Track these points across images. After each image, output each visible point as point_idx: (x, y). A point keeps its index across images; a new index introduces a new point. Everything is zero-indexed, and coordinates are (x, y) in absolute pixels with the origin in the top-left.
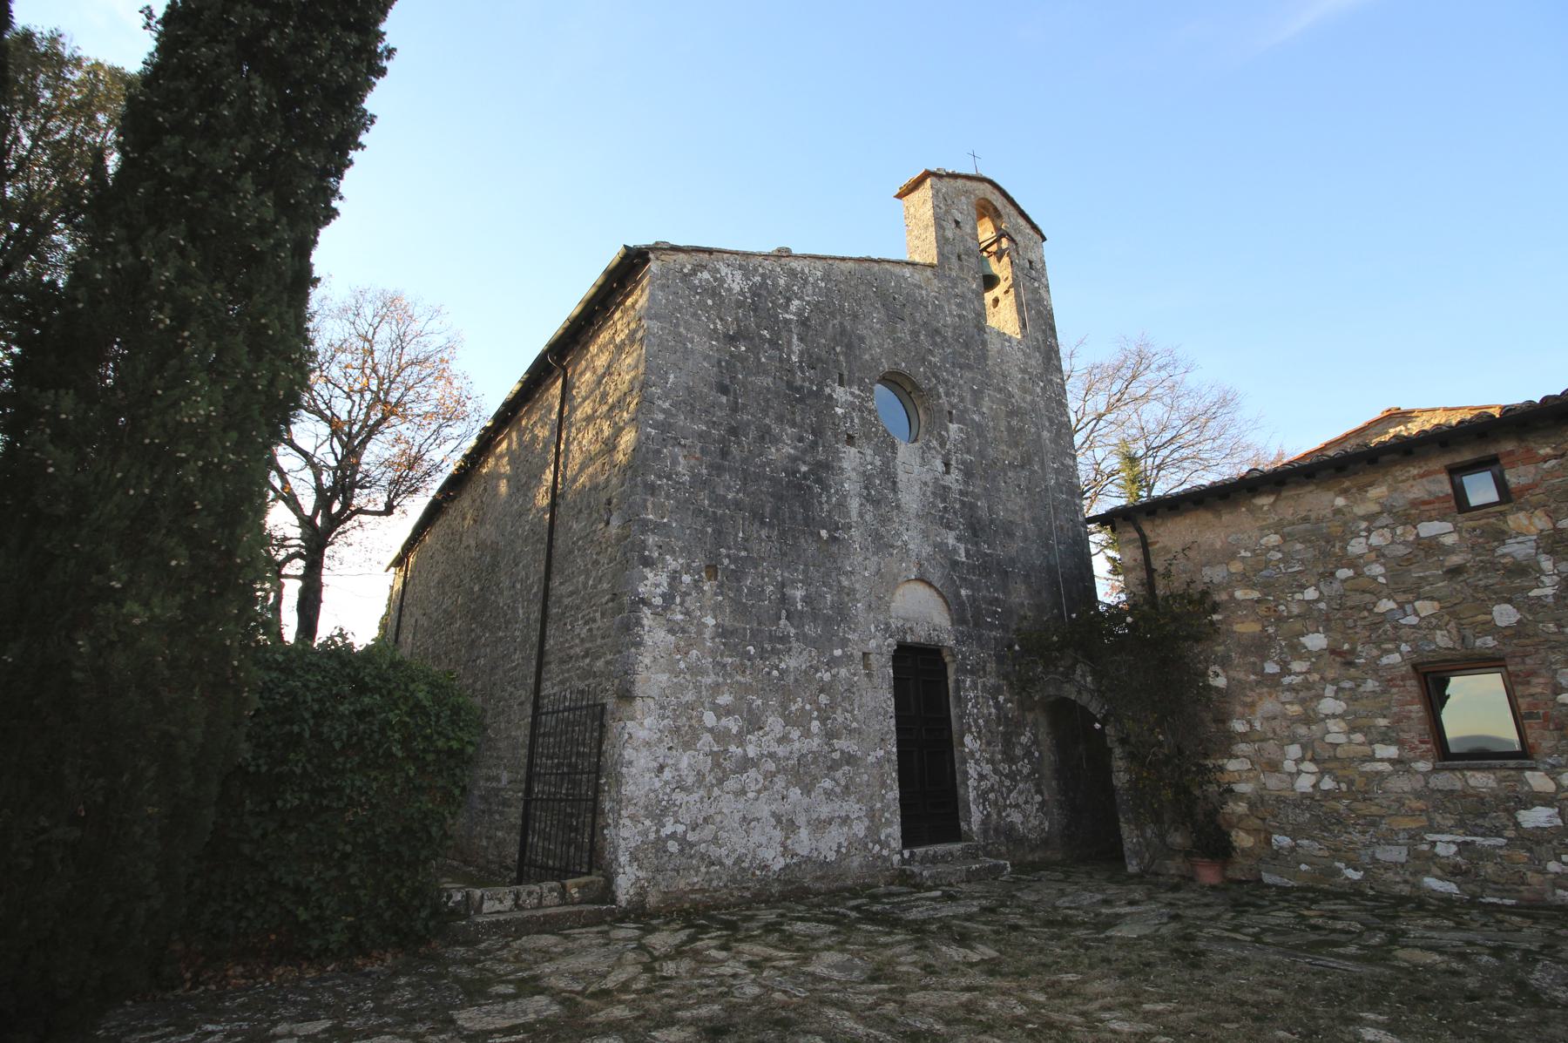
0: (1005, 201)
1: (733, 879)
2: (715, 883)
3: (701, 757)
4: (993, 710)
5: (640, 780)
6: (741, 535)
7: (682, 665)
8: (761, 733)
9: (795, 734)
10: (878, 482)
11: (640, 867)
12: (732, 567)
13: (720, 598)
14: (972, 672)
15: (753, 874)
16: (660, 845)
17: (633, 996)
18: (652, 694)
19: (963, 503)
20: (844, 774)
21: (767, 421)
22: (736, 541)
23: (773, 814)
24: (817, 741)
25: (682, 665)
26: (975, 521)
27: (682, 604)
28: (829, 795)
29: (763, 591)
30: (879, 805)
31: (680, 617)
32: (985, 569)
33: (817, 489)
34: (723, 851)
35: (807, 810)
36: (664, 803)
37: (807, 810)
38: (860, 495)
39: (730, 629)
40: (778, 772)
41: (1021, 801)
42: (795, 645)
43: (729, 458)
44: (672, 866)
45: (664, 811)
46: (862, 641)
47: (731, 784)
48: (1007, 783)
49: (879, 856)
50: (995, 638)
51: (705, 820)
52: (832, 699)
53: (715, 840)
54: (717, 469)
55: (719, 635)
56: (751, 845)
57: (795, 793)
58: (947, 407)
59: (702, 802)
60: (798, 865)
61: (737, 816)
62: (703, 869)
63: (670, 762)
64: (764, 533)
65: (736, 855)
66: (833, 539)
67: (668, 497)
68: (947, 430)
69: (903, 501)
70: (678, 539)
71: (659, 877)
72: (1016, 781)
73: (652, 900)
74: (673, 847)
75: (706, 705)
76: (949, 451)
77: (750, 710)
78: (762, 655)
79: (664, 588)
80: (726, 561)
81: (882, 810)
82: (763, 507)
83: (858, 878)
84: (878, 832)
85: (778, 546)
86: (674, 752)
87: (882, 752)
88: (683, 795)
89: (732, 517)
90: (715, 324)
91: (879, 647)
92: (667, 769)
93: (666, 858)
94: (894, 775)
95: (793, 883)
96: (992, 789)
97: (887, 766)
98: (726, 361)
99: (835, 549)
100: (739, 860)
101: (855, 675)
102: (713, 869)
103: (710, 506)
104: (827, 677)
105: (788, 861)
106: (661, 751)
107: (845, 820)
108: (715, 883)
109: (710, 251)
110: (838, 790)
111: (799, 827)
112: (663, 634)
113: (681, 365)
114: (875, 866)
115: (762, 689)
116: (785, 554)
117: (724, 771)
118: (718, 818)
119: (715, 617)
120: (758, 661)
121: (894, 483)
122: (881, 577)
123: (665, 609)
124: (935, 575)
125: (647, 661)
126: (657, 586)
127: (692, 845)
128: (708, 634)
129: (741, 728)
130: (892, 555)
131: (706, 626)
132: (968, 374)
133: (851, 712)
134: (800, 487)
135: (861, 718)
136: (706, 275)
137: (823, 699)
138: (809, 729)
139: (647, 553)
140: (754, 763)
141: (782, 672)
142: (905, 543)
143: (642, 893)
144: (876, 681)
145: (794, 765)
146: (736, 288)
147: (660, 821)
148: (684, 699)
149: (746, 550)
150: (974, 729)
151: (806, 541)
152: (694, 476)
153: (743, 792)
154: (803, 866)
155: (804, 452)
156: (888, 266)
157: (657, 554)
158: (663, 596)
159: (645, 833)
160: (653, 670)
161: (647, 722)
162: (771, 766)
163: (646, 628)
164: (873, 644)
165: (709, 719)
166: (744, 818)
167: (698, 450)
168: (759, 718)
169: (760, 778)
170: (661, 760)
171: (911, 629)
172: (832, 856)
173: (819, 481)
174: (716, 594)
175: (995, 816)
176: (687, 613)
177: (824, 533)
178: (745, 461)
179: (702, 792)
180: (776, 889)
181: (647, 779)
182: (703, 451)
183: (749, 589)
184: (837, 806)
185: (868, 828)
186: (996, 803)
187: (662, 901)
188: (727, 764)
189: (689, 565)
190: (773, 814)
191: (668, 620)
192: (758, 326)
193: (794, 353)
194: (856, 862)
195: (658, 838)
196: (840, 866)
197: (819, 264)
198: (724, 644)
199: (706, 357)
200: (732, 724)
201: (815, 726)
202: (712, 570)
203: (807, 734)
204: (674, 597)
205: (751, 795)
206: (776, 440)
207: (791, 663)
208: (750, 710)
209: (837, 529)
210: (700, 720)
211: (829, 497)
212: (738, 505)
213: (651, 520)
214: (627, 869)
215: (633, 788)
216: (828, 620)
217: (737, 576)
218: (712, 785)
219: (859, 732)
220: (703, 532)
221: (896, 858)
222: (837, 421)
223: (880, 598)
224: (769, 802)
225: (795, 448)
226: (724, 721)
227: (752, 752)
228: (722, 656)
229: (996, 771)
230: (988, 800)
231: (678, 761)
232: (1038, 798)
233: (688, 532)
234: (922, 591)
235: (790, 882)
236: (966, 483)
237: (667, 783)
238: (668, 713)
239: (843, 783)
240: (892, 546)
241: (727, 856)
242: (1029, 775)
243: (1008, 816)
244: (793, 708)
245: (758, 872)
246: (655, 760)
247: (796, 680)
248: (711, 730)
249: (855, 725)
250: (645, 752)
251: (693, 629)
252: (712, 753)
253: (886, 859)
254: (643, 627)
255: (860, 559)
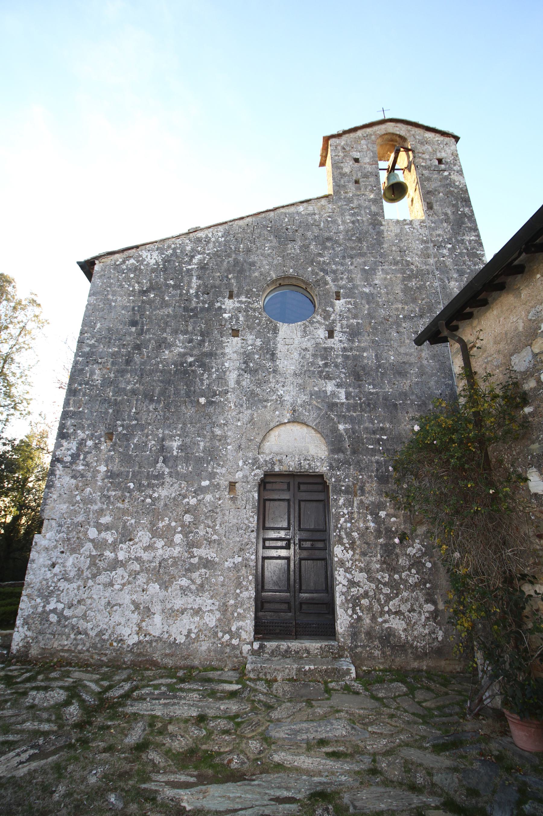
0: (409, 127)
1: (94, 646)
2: (80, 647)
3: (82, 558)
4: (372, 525)
5: (38, 572)
6: (134, 410)
7: (78, 498)
8: (131, 543)
9: (160, 543)
10: (257, 356)
11: (29, 629)
12: (125, 432)
13: (112, 453)
14: (347, 492)
15: (111, 645)
16: (44, 616)
17: (151, 683)
18: (54, 517)
19: (346, 357)
20: (200, 575)
21: (165, 335)
22: (129, 415)
23: (133, 602)
24: (178, 549)
25: (78, 498)
26: (358, 369)
27: (84, 460)
28: (185, 591)
29: (146, 445)
30: (232, 602)
31: (81, 467)
32: (369, 405)
33: (200, 371)
34: (90, 625)
35: (163, 601)
36: (51, 588)
37: (163, 601)
38: (239, 369)
39: (117, 472)
40: (142, 571)
41: (404, 608)
42: (168, 479)
43: (132, 364)
44: (50, 631)
45: (51, 593)
46: (230, 473)
47: (103, 578)
48: (386, 590)
49: (228, 644)
50: (377, 462)
51: (79, 602)
52: (195, 518)
53: (84, 617)
54: (122, 372)
55: (107, 477)
56: (112, 623)
57: (154, 588)
58: (334, 289)
59: (78, 589)
60: (150, 642)
61: (103, 602)
62: (72, 636)
63: (60, 561)
64: (151, 408)
65: (98, 629)
66: (210, 403)
67: (84, 395)
68: (333, 306)
69: (281, 366)
70: (87, 419)
71: (40, 638)
72: (398, 589)
73: (34, 652)
74: (53, 618)
75: (92, 523)
76: (334, 321)
77: (124, 527)
78: (140, 488)
79: (74, 450)
80: (120, 429)
81: (236, 606)
82: (153, 390)
83: (206, 659)
84: (229, 624)
85: (161, 413)
86: (64, 555)
87: (240, 559)
88: (66, 583)
89: (128, 401)
90: (134, 287)
91: (245, 477)
92: (57, 566)
93: (47, 625)
94: (251, 578)
95: (145, 656)
96: (366, 595)
97: (243, 571)
98: (139, 307)
99: (211, 409)
100: (101, 633)
101: (220, 499)
102: (80, 637)
103: (113, 396)
104: (193, 501)
105: (141, 638)
106: (55, 554)
107: (198, 612)
108: (80, 647)
109: (137, 247)
110: (193, 587)
111: (154, 614)
112: (68, 479)
113: (106, 317)
114: (222, 652)
115: (137, 512)
116: (168, 418)
117: (98, 569)
118: (89, 601)
119: (107, 466)
120: (136, 493)
121: (273, 355)
122: (254, 424)
123: (71, 463)
124: (311, 416)
125: (55, 497)
126: (69, 450)
127: (67, 618)
128: (99, 477)
129: (116, 540)
130: (266, 407)
131: (98, 471)
132: (360, 260)
133: (213, 528)
134: (186, 372)
135: (221, 532)
136: (132, 261)
137: (188, 518)
138: (172, 541)
139: (65, 431)
140: (123, 564)
141: (154, 500)
142: (281, 397)
143: (27, 646)
144: (239, 503)
145: (155, 568)
146: (153, 261)
147: (47, 600)
148: (76, 520)
149: (136, 420)
150: (345, 541)
151: (186, 407)
152: (104, 379)
153: (111, 584)
154: (154, 644)
155: (192, 349)
156: (282, 210)
157: (72, 430)
158: (72, 456)
159: (36, 607)
160: (58, 502)
161: (48, 535)
162: (136, 567)
163: (57, 476)
164: (239, 475)
165: (93, 533)
166: (109, 603)
167: (109, 364)
168: (131, 533)
169: (126, 575)
170: (54, 560)
171: (280, 461)
172: (181, 639)
173: (203, 365)
174: (110, 451)
175: (367, 621)
176: (87, 465)
177: (202, 400)
178: (143, 364)
179: (80, 583)
180: (128, 658)
181: (42, 571)
182: (113, 364)
183: (135, 445)
184: (190, 600)
185: (219, 620)
186: (370, 608)
187: (40, 654)
188: (101, 564)
189: (92, 435)
190: (133, 602)
191: (73, 470)
192: (166, 279)
193: (191, 288)
194: (204, 646)
195: (44, 611)
196: (188, 648)
197: (221, 228)
198: (111, 483)
199: (124, 308)
200: (109, 537)
201: (178, 538)
202: (109, 436)
203: (170, 543)
204: (79, 455)
205: (117, 587)
206: (169, 346)
207: (163, 492)
208: (124, 527)
209: (215, 395)
210: (86, 534)
211: (210, 375)
212: (134, 392)
213: (70, 411)
214: (20, 629)
215: (32, 577)
216: (199, 460)
217: (127, 438)
218: (88, 578)
219: (219, 543)
220: (106, 413)
221: (246, 648)
222: (223, 323)
223: (250, 440)
224: (130, 593)
225: (185, 347)
226: (103, 535)
227: (121, 556)
228: (108, 491)
229: (371, 579)
230: (360, 606)
231: (66, 560)
232: (430, 607)
233: (95, 414)
234: (298, 430)
235: (139, 655)
236: (351, 341)
237: (55, 575)
238: (64, 529)
239: (198, 581)
240: (267, 401)
241: (92, 629)
242: (416, 585)
243: (385, 621)
244: (161, 525)
245: (115, 644)
246: (50, 560)
247: (166, 505)
248: (92, 541)
249: (215, 537)
250: (44, 554)
251: (89, 475)
252: (90, 556)
253: (234, 647)
254: (55, 475)
255: (234, 413)
